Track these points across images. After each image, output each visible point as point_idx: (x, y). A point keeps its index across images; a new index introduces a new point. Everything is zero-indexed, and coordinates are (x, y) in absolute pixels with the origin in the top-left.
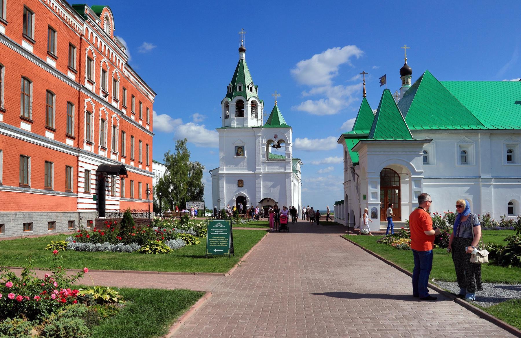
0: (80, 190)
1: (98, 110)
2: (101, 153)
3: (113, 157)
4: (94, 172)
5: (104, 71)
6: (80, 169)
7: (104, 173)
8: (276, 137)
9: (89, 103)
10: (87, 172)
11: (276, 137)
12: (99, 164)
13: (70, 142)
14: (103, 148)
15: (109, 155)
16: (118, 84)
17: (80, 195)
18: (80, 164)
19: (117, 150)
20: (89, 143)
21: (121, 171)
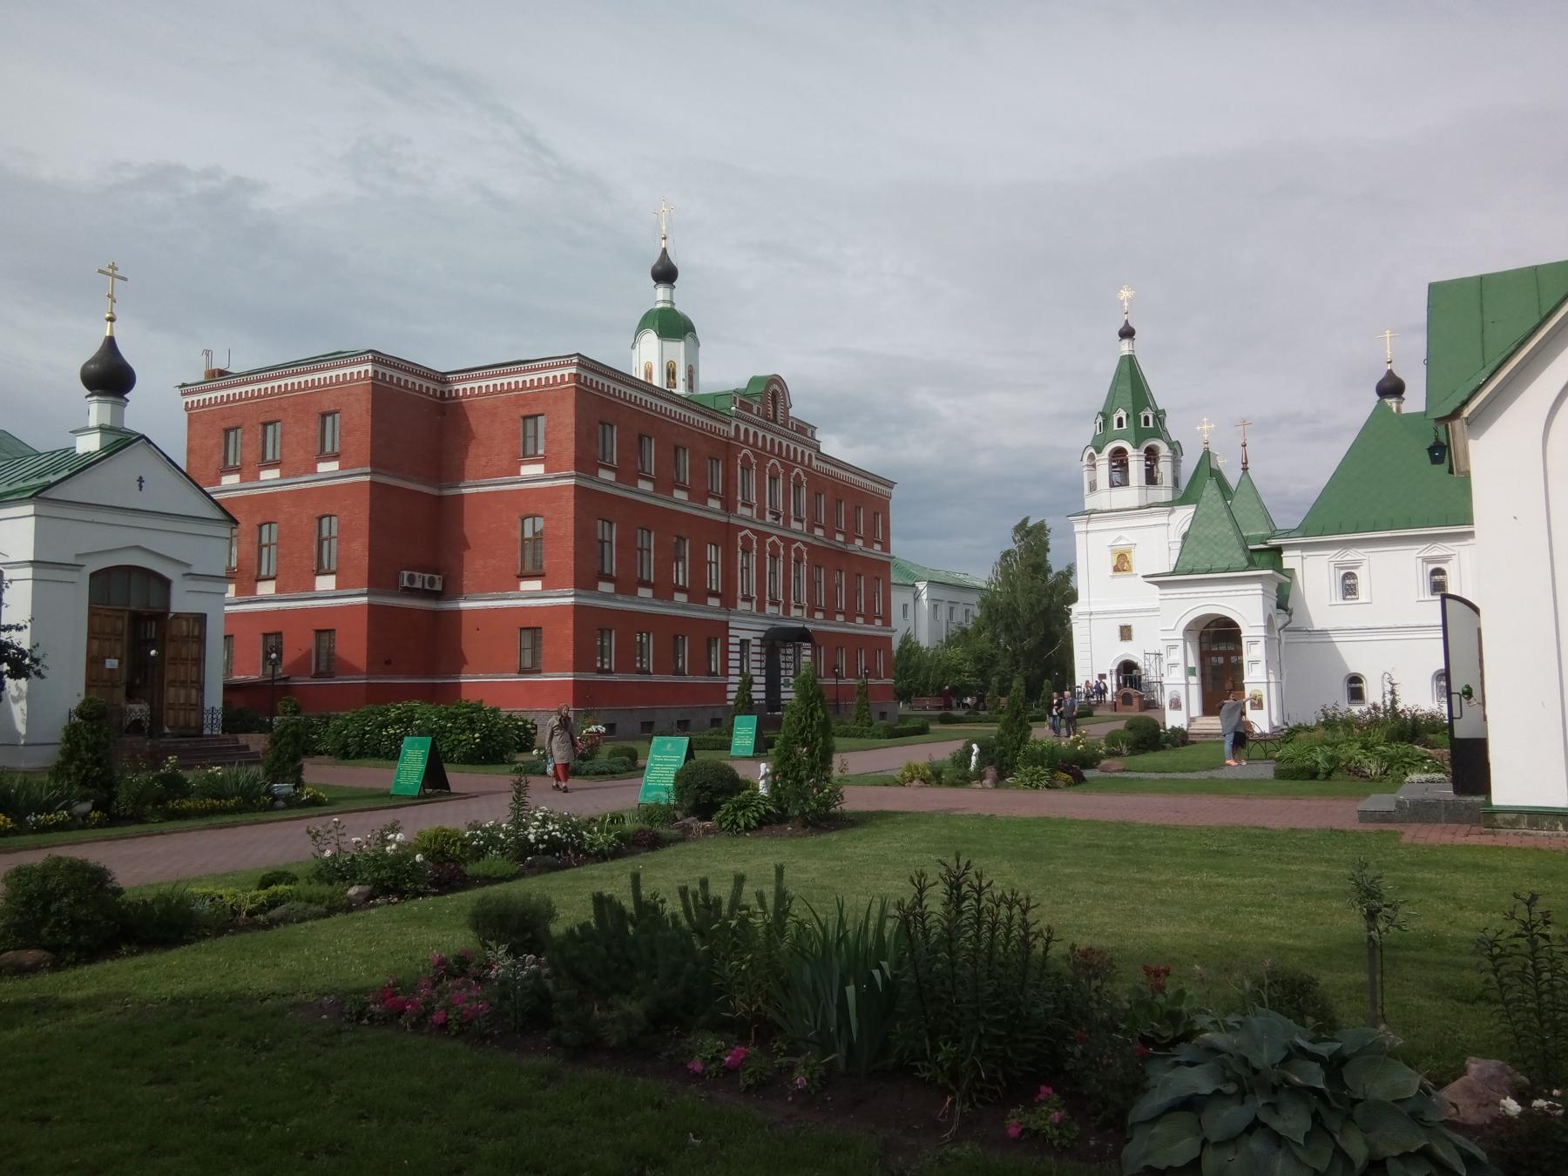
0: (731, 671)
1: (761, 544)
2: (769, 609)
3: (794, 612)
4: (758, 642)
5: (773, 479)
6: (731, 640)
7: (777, 641)
9: (745, 538)
10: (744, 644)
12: (766, 628)
13: (714, 602)
14: (774, 603)
15: (787, 611)
16: (804, 491)
17: (731, 679)
18: (731, 632)
19: (804, 602)
20: (747, 599)
21: (803, 635)
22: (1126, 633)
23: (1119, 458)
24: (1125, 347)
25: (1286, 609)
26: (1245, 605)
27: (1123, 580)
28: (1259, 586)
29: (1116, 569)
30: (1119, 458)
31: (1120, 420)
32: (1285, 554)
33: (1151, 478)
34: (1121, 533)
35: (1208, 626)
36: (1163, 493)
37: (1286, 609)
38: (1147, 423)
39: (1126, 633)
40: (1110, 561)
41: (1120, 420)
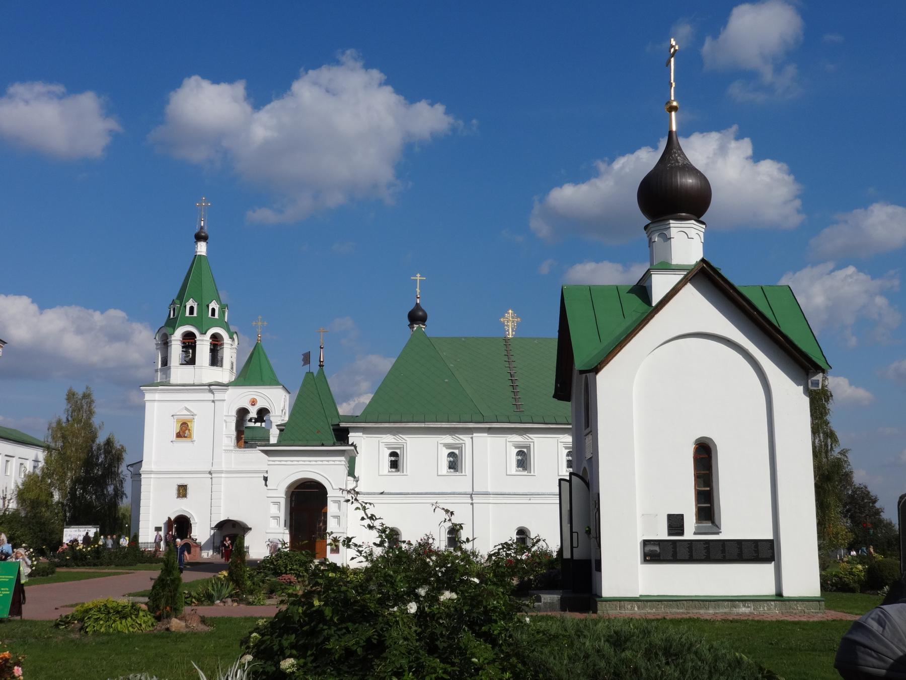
8: (253, 403)
11: (253, 403)
22: (182, 491)
23: (189, 342)
24: (202, 248)
25: (354, 477)
26: (326, 470)
27: (183, 444)
28: (343, 458)
29: (179, 435)
30: (189, 342)
31: (192, 309)
32: (351, 435)
33: (215, 360)
34: (187, 405)
35: (297, 488)
36: (224, 374)
37: (354, 477)
38: (213, 314)
39: (182, 491)
40: (175, 428)
41: (192, 309)
